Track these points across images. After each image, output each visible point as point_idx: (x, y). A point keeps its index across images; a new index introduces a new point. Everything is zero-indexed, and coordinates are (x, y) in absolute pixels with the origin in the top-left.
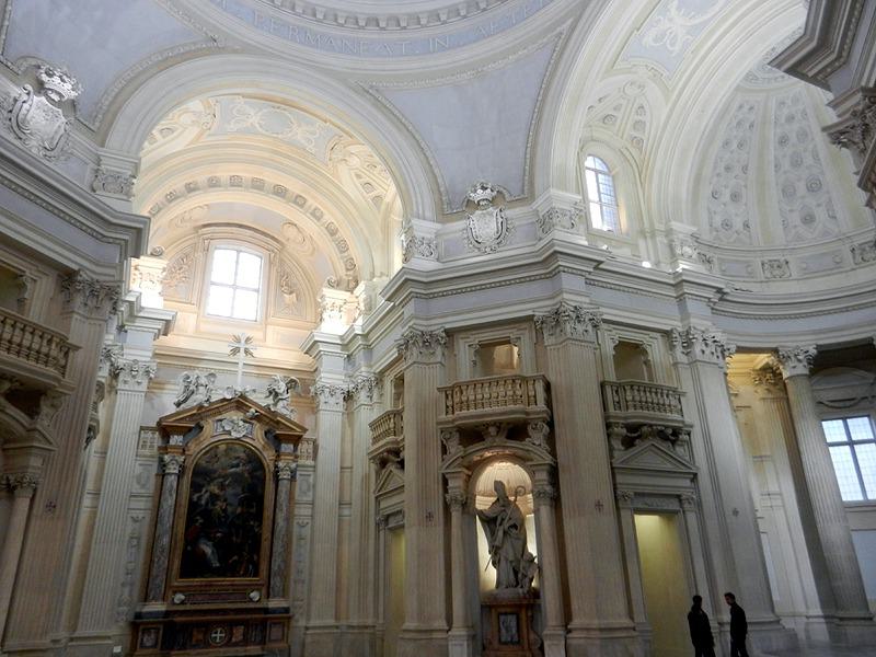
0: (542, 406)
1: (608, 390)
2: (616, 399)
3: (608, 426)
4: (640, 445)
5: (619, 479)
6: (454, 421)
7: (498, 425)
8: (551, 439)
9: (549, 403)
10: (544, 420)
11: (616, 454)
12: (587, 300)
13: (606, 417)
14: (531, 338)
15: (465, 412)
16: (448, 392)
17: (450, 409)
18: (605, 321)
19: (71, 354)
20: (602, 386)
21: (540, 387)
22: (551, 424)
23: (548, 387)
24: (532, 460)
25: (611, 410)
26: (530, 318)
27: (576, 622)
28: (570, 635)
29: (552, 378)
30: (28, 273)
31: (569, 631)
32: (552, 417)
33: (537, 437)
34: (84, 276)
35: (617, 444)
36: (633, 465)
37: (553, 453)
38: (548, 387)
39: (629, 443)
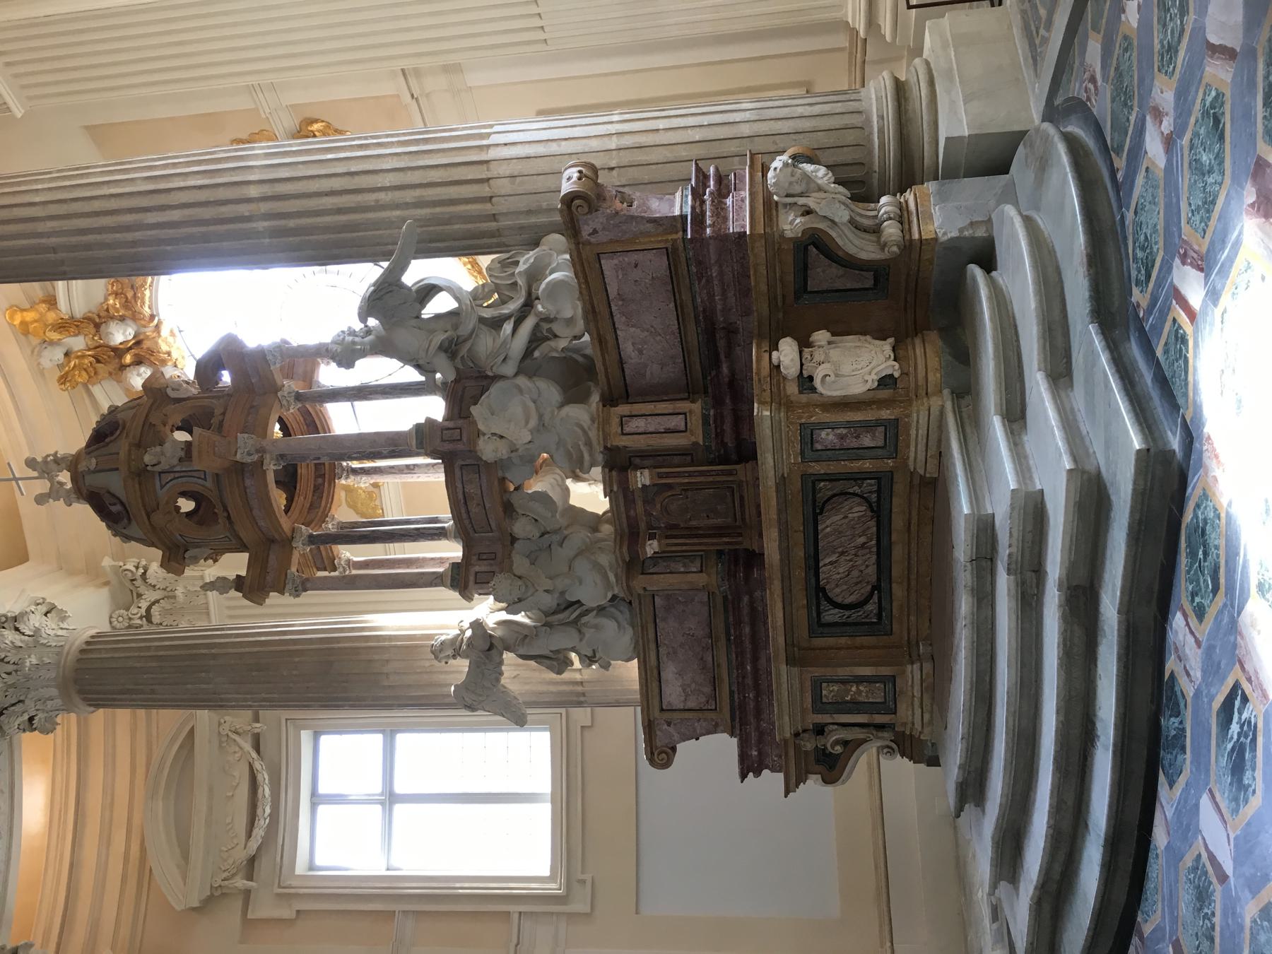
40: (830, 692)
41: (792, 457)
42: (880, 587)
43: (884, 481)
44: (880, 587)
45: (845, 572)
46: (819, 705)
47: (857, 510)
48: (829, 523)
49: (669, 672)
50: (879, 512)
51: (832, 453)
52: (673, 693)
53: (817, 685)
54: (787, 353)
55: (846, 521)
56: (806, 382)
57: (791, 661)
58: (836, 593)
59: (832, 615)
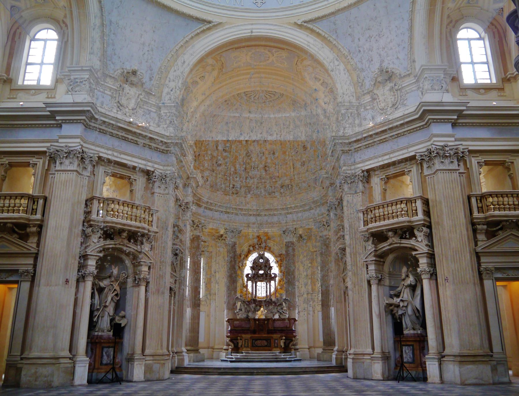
0: (421, 215)
1: (473, 200)
2: (480, 205)
3: (473, 224)
4: (501, 235)
5: (483, 259)
6: (368, 229)
7: (395, 231)
8: (430, 236)
9: (427, 213)
10: (424, 225)
11: (480, 244)
12: (453, 139)
13: (472, 219)
14: (417, 171)
15: (374, 225)
16: (366, 212)
17: (366, 223)
18: (470, 152)
19: (154, 215)
20: (469, 198)
21: (419, 204)
22: (430, 227)
23: (426, 202)
24: (416, 250)
25: (476, 214)
26: (413, 158)
27: (447, 351)
28: (442, 359)
29: (430, 196)
30: (132, 177)
31: (444, 357)
32: (430, 223)
33: (420, 236)
34: (157, 173)
35: (481, 237)
36: (495, 249)
37: (431, 246)
38: (426, 202)
39: (490, 235)
40: (247, 341)
41: (275, 338)
42: (257, 346)
43: (270, 346)
44: (257, 346)
45: (258, 342)
46: (245, 339)
47: (266, 344)
48: (265, 341)
49: (238, 322)
50: (266, 346)
51: (275, 342)
52: (236, 322)
53: (248, 340)
54: (284, 338)
55: (265, 343)
56: (282, 339)
57: (251, 337)
58: (256, 342)
59: (254, 341)
